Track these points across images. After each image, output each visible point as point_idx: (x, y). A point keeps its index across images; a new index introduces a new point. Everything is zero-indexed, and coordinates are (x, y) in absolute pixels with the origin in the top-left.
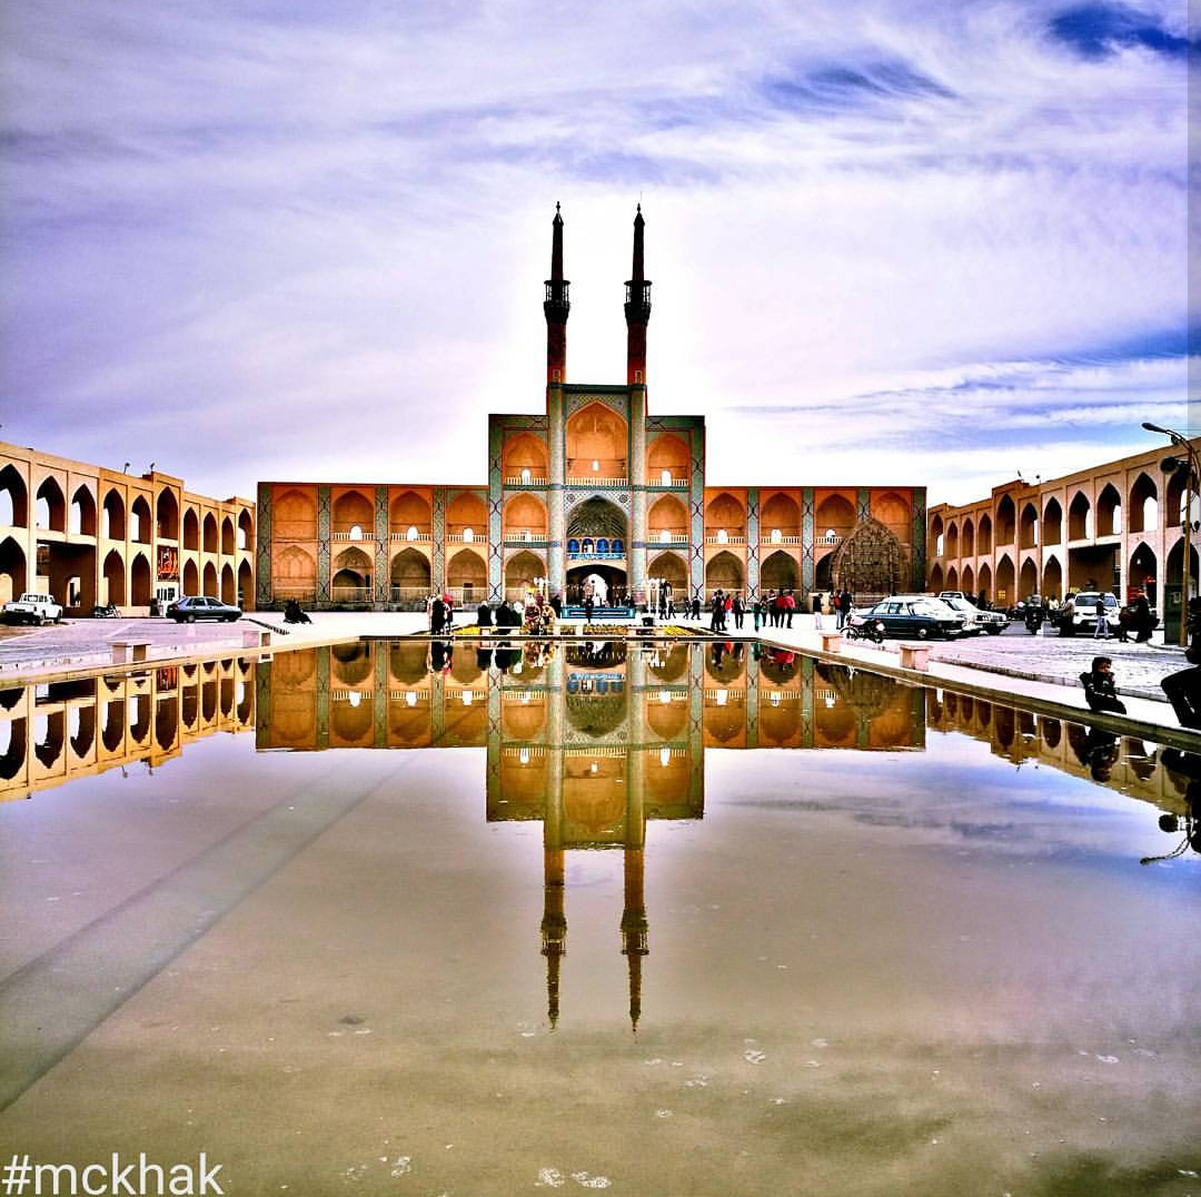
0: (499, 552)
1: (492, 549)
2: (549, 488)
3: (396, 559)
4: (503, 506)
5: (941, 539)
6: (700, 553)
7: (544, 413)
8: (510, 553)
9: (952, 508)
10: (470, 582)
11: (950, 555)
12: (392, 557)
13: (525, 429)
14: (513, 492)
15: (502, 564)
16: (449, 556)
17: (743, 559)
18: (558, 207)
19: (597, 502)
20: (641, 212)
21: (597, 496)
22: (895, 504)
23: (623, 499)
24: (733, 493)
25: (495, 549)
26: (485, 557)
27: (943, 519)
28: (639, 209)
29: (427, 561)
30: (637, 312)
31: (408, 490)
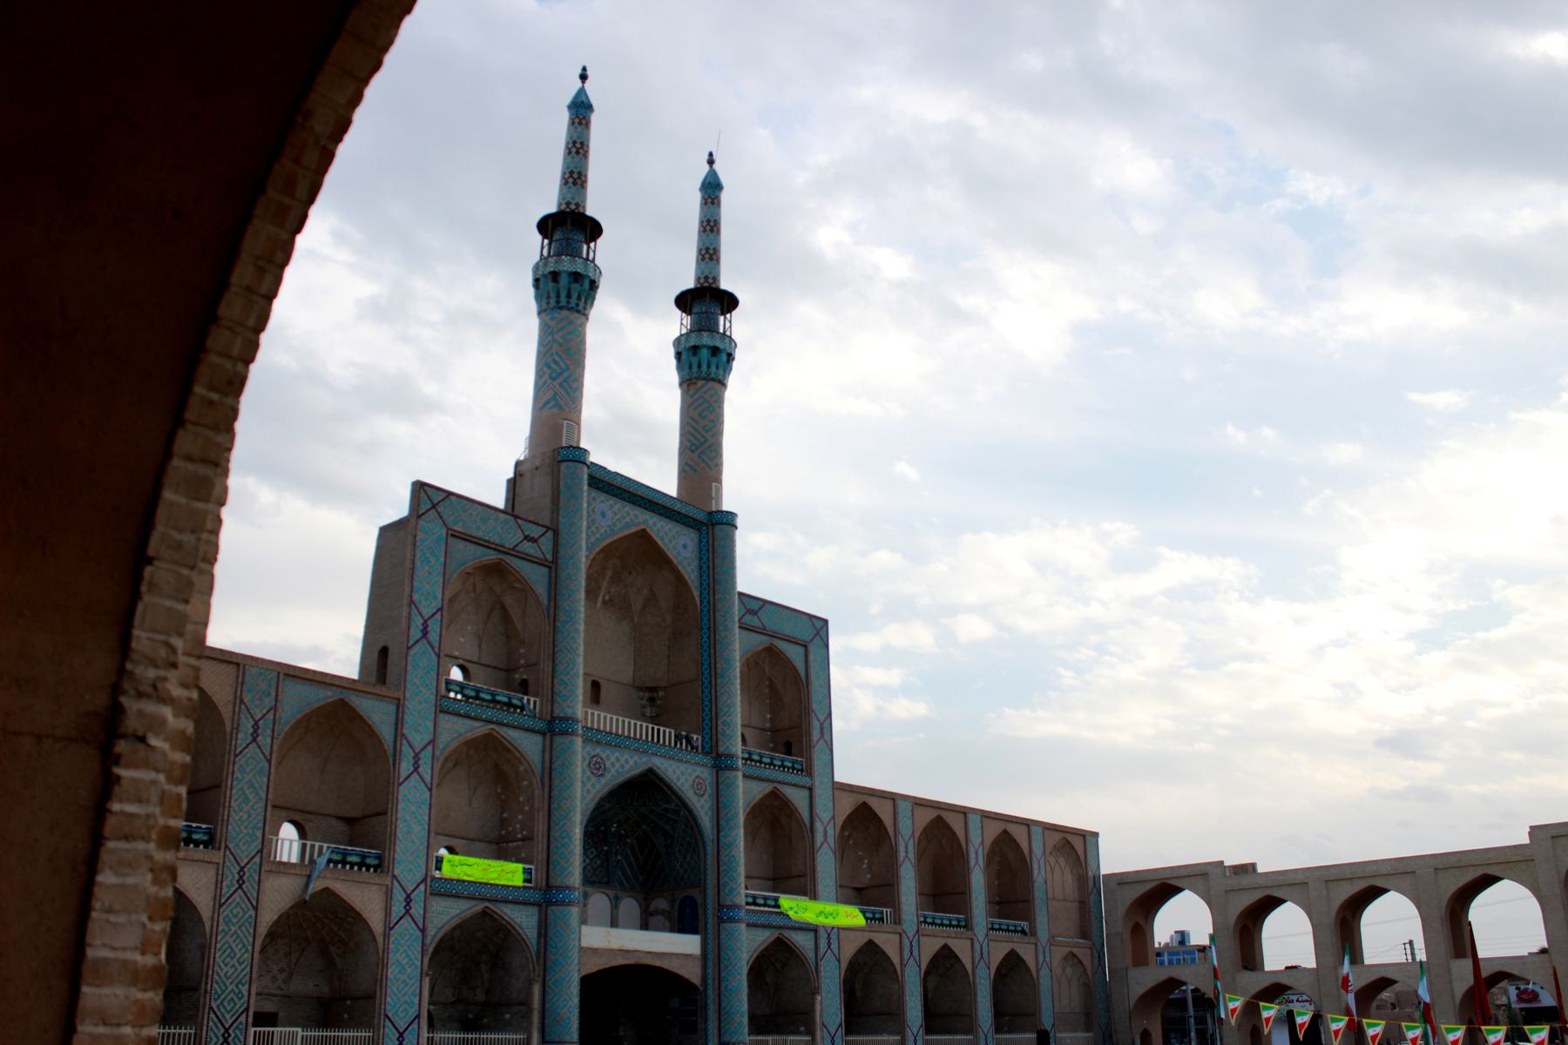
0: (417, 910)
1: (399, 896)
6: (834, 946)
8: (446, 914)
10: (269, 1007)
16: (268, 916)
17: (896, 960)
18: (584, 77)
19: (647, 786)
21: (650, 772)
23: (698, 786)
24: (874, 803)
25: (408, 900)
26: (375, 920)
28: (711, 162)
30: (704, 363)
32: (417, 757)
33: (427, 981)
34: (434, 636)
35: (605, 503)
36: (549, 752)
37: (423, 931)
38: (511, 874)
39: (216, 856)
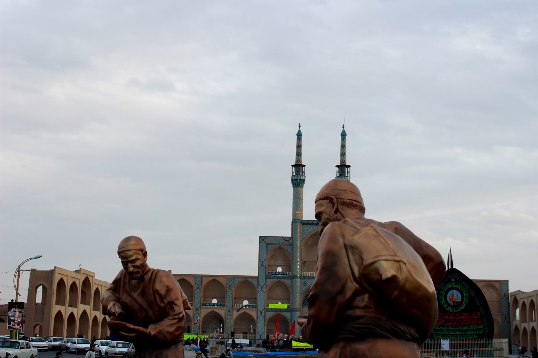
0: (263, 314)
1: (259, 312)
2: (293, 278)
3: (205, 317)
4: (266, 287)
5: (518, 311)
7: (290, 236)
8: (269, 315)
9: (523, 293)
10: (246, 331)
11: (523, 319)
12: (203, 315)
13: (279, 244)
14: (272, 280)
15: (265, 322)
18: (300, 126)
20: (345, 129)
22: (491, 290)
25: (261, 313)
26: (255, 316)
27: (518, 300)
28: (343, 127)
29: (222, 318)
31: (212, 278)
32: (262, 287)
33: (266, 327)
34: (264, 265)
35: (307, 227)
36: (292, 282)
37: (264, 318)
38: (285, 306)
39: (225, 308)
